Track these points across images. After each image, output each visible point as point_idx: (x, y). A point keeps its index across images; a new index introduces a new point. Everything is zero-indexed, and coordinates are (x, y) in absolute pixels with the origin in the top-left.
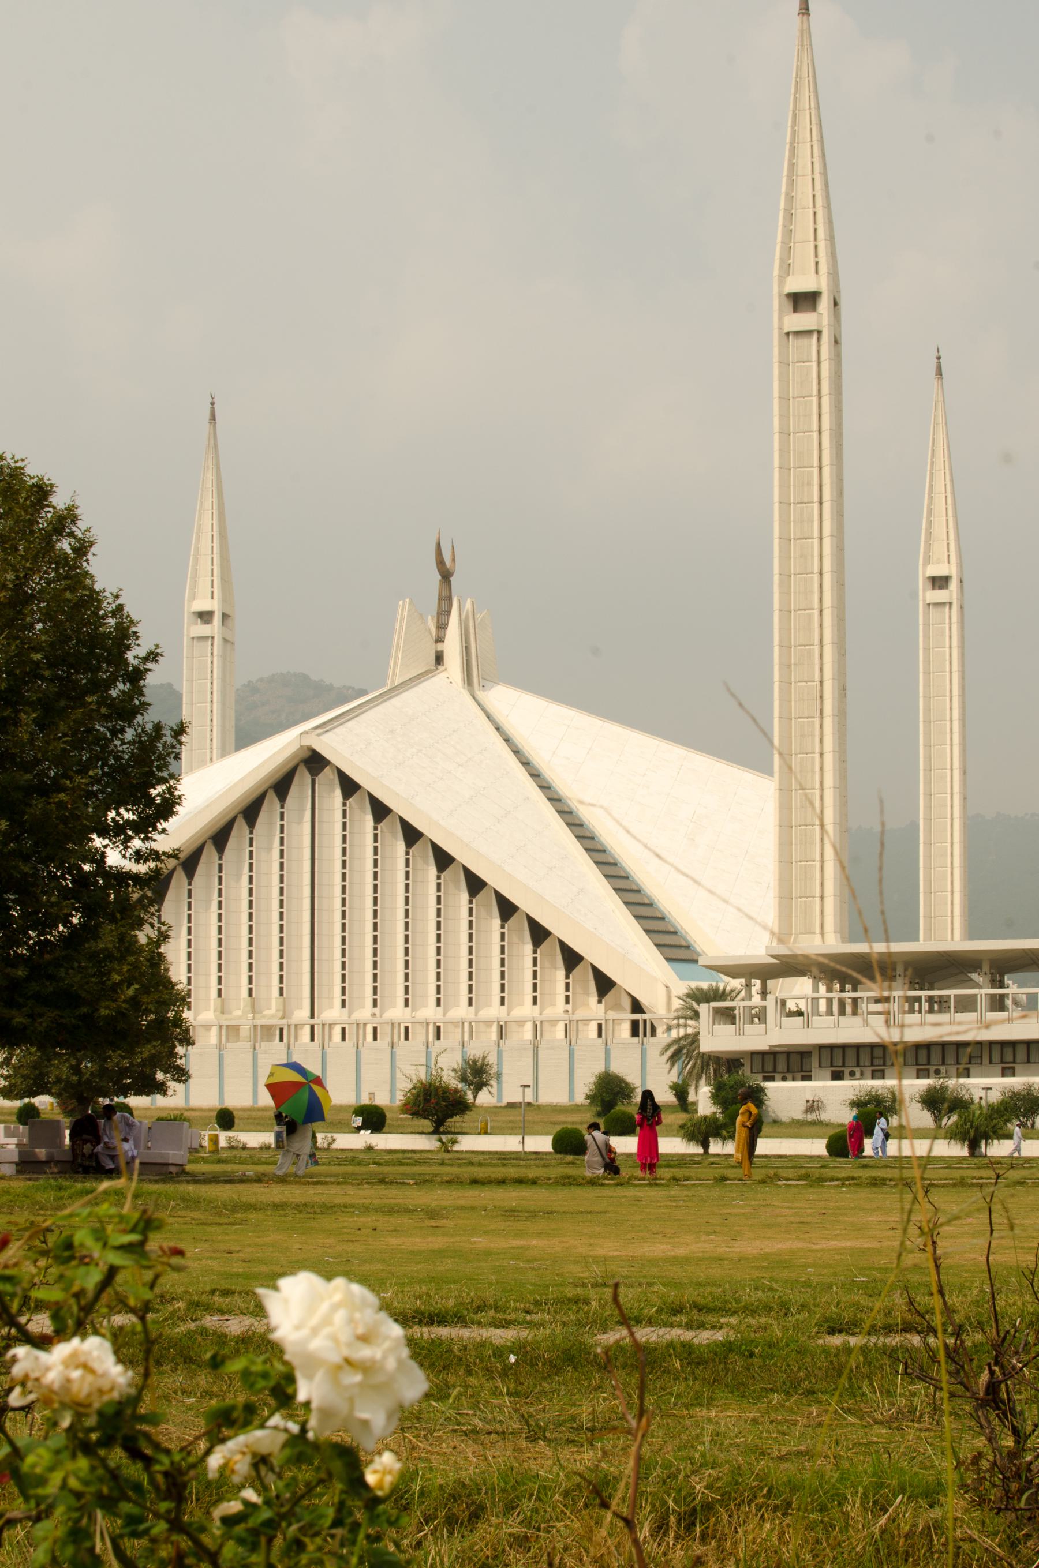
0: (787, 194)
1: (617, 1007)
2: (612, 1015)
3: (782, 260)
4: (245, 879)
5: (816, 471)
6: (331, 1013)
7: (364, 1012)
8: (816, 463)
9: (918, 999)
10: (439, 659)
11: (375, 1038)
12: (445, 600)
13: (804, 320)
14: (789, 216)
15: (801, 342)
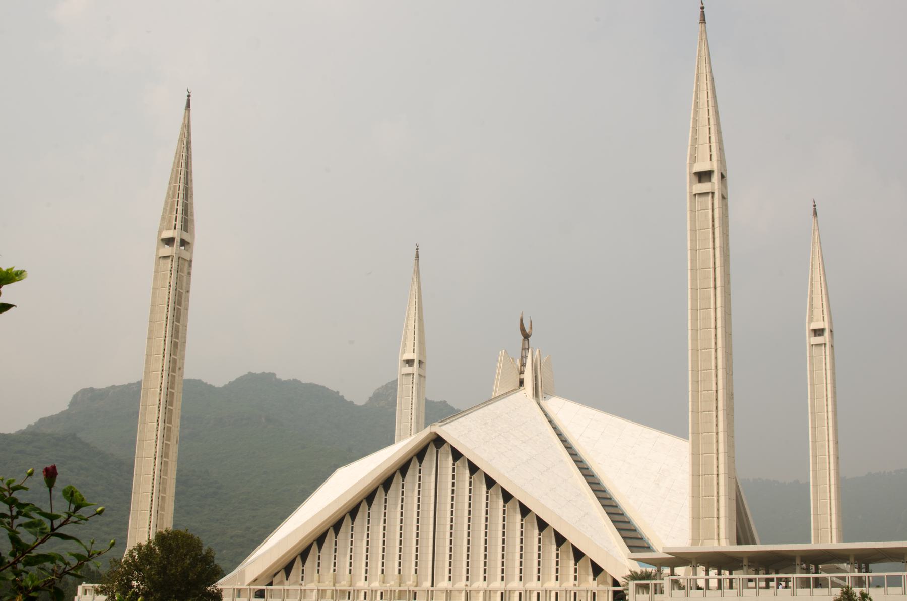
0: (694, 119)
1: (604, 582)
2: (601, 587)
3: (691, 155)
4: (399, 507)
5: (712, 270)
6: (443, 584)
7: (461, 584)
8: (712, 266)
9: (772, 580)
10: (521, 383)
11: (382, 598)
12: (526, 349)
13: (705, 187)
14: (695, 130)
15: (703, 199)
